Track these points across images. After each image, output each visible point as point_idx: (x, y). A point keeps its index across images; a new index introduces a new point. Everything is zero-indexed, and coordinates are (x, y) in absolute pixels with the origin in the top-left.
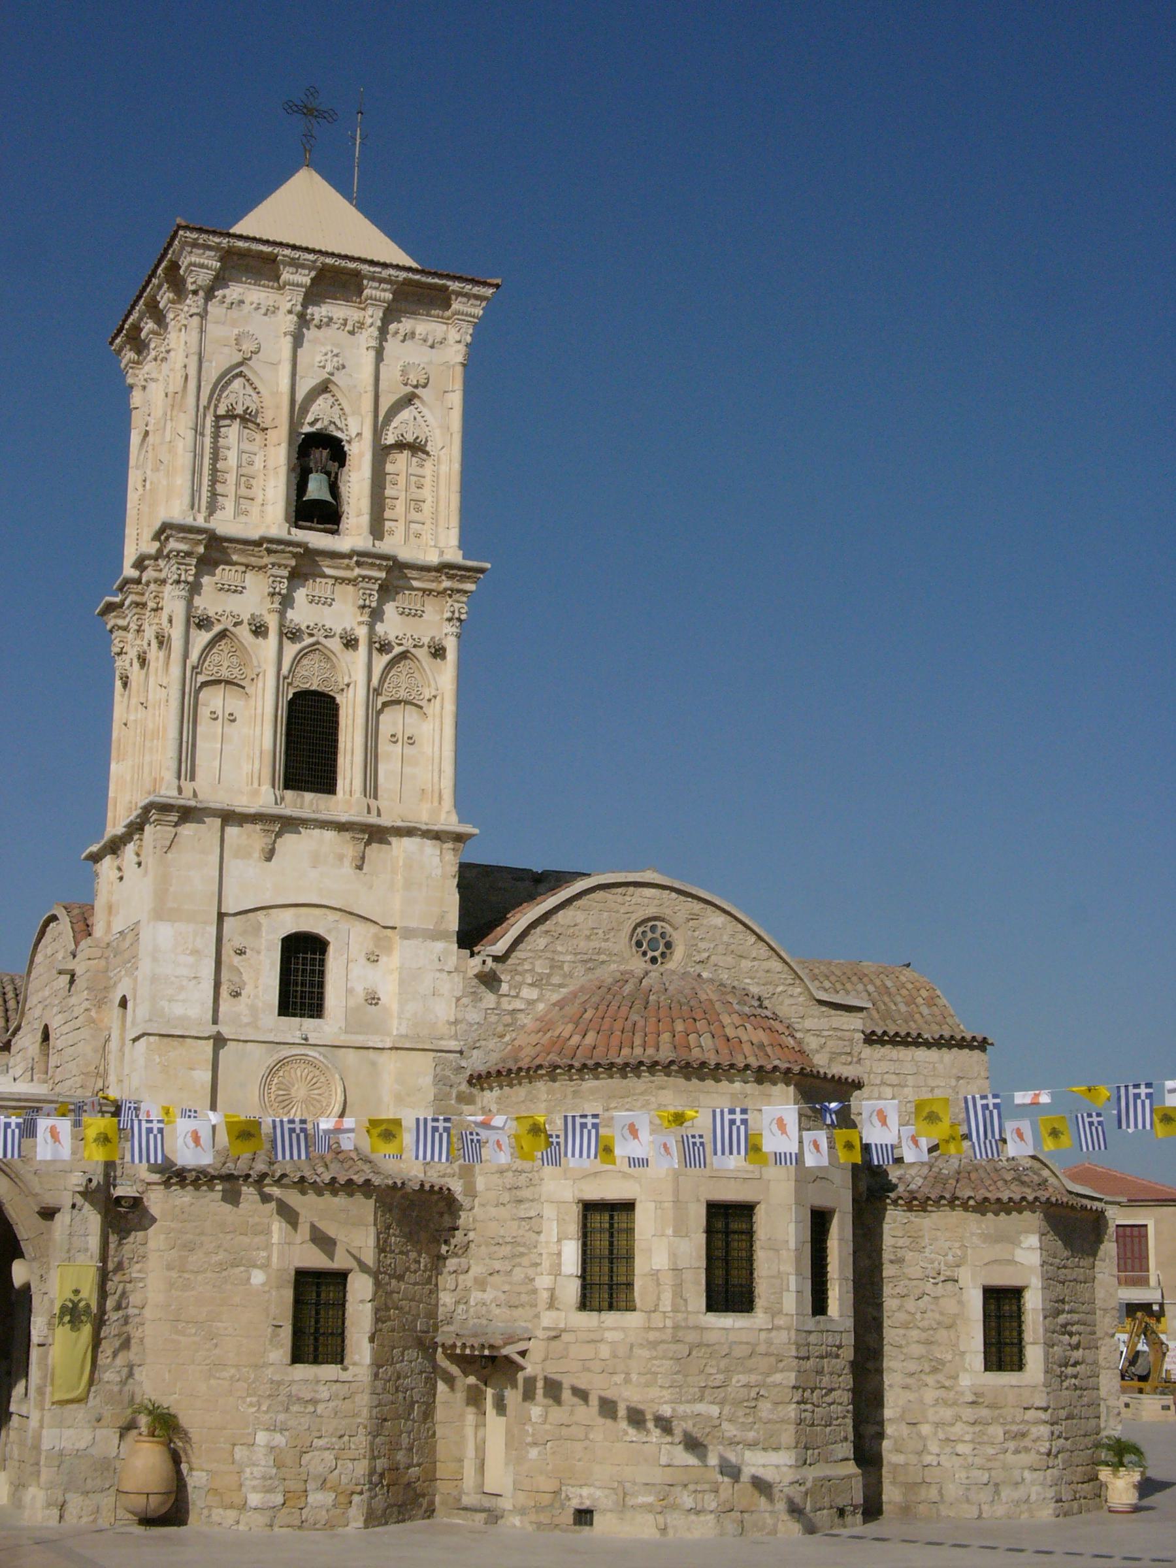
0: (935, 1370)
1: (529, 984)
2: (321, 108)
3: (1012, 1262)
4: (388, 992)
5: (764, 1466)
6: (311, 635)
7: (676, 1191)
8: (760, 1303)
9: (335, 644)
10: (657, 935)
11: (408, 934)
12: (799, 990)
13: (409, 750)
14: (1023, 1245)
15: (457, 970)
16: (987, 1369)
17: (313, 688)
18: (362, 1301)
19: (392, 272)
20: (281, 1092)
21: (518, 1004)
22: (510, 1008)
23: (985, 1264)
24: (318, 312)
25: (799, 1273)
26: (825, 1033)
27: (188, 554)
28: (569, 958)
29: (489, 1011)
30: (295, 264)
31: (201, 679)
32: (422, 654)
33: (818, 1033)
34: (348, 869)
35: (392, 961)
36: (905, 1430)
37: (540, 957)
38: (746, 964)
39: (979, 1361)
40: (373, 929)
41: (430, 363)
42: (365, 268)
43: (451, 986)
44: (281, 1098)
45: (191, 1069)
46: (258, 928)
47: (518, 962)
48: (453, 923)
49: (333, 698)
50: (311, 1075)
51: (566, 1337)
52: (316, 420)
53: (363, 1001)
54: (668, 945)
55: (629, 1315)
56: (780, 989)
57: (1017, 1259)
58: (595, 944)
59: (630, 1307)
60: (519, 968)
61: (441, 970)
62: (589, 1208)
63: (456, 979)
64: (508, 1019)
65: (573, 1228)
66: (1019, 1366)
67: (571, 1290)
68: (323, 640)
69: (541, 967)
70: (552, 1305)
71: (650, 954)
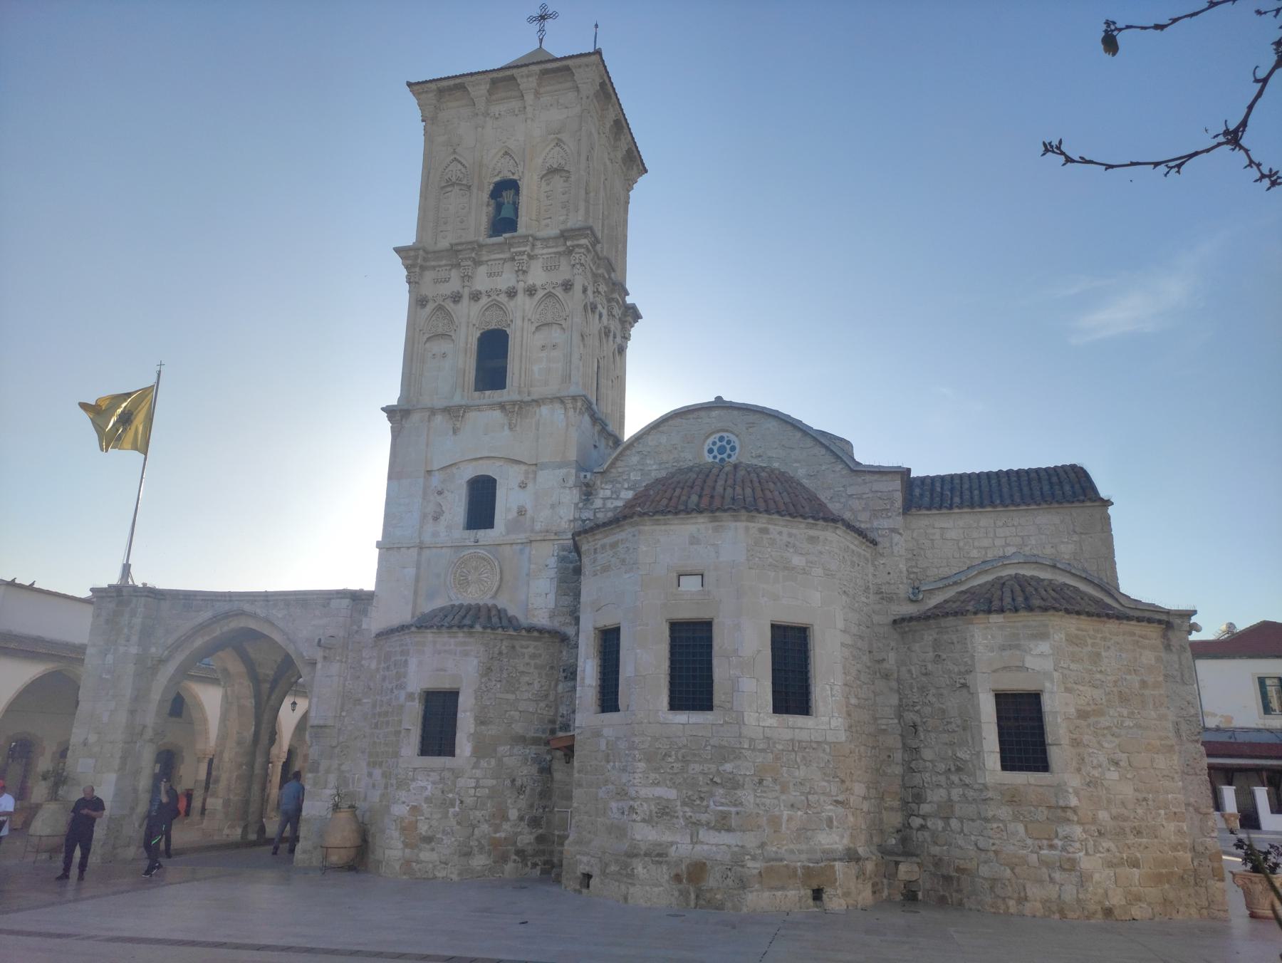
0: (959, 769)
1: (626, 489)
2: (549, 13)
3: (1022, 668)
5: (717, 845)
6: (489, 296)
8: (716, 701)
9: (503, 298)
10: (724, 443)
12: (841, 466)
14: (1034, 652)
15: (575, 486)
17: (493, 327)
18: (465, 711)
20: (462, 578)
22: (612, 506)
23: (994, 671)
24: (496, 109)
26: (865, 496)
28: (654, 467)
29: (597, 510)
31: (427, 336)
32: (559, 292)
33: (859, 496)
34: (507, 432)
36: (940, 824)
37: (634, 469)
40: (524, 468)
41: (568, 117)
42: (514, 71)
44: (462, 582)
45: (404, 568)
47: (618, 475)
49: (505, 331)
50: (482, 565)
52: (500, 172)
53: (516, 514)
54: (733, 449)
56: (823, 468)
57: (1027, 665)
60: (620, 479)
61: (565, 487)
63: (575, 492)
68: (496, 298)
71: (719, 457)
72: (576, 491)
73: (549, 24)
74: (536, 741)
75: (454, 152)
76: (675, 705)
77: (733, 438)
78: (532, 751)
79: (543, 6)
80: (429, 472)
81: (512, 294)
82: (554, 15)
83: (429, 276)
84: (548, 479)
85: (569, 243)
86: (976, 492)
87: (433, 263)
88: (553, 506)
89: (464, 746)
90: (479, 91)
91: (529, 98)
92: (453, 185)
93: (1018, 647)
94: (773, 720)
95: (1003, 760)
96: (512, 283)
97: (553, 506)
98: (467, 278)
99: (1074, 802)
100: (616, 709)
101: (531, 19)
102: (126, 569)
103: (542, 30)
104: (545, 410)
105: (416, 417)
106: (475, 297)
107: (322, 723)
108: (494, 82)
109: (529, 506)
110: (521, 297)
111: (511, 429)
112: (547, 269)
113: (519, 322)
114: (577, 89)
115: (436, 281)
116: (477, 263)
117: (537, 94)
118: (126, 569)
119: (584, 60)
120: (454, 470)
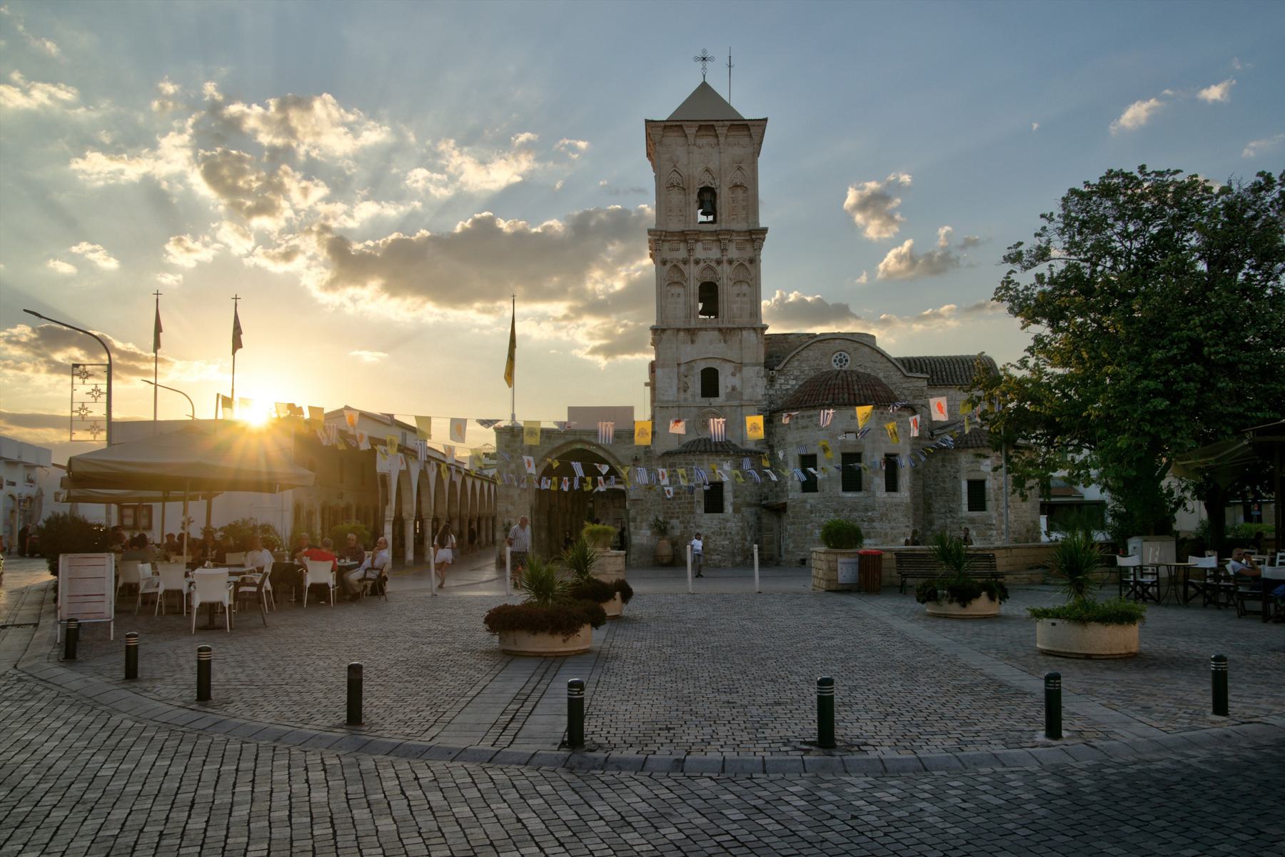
0: (950, 511)
3: (979, 471)
8: (863, 487)
9: (713, 264)
11: (746, 365)
13: (745, 299)
15: (765, 376)
16: (969, 510)
19: (725, 122)
21: (789, 387)
24: (701, 141)
27: (658, 240)
30: (687, 126)
34: (723, 344)
38: (878, 365)
39: (965, 508)
40: (733, 364)
46: (693, 367)
54: (846, 361)
55: (816, 494)
58: (817, 362)
59: (817, 491)
65: (798, 464)
66: (983, 508)
72: (765, 379)
73: (709, 64)
74: (755, 505)
75: (675, 166)
76: (844, 490)
77: (846, 355)
78: (753, 509)
79: (704, 51)
80: (679, 365)
81: (719, 262)
82: (712, 59)
83: (666, 246)
84: (749, 372)
85: (754, 237)
86: (944, 373)
87: (669, 238)
88: (753, 387)
89: (729, 508)
90: (691, 131)
91: (722, 139)
92: (674, 186)
93: (978, 462)
94: (885, 495)
95: (969, 507)
96: (719, 256)
97: (753, 387)
98: (690, 250)
99: (994, 522)
101: (696, 59)
102: (513, 416)
103: (704, 68)
104: (745, 333)
105: (669, 332)
106: (697, 262)
107: (636, 498)
108: (700, 127)
109: (738, 386)
110: (725, 265)
111: (725, 342)
112: (739, 249)
113: (725, 280)
114: (750, 136)
115: (671, 250)
116: (697, 241)
117: (727, 136)
118: (513, 416)
119: (757, 123)
120: (693, 364)
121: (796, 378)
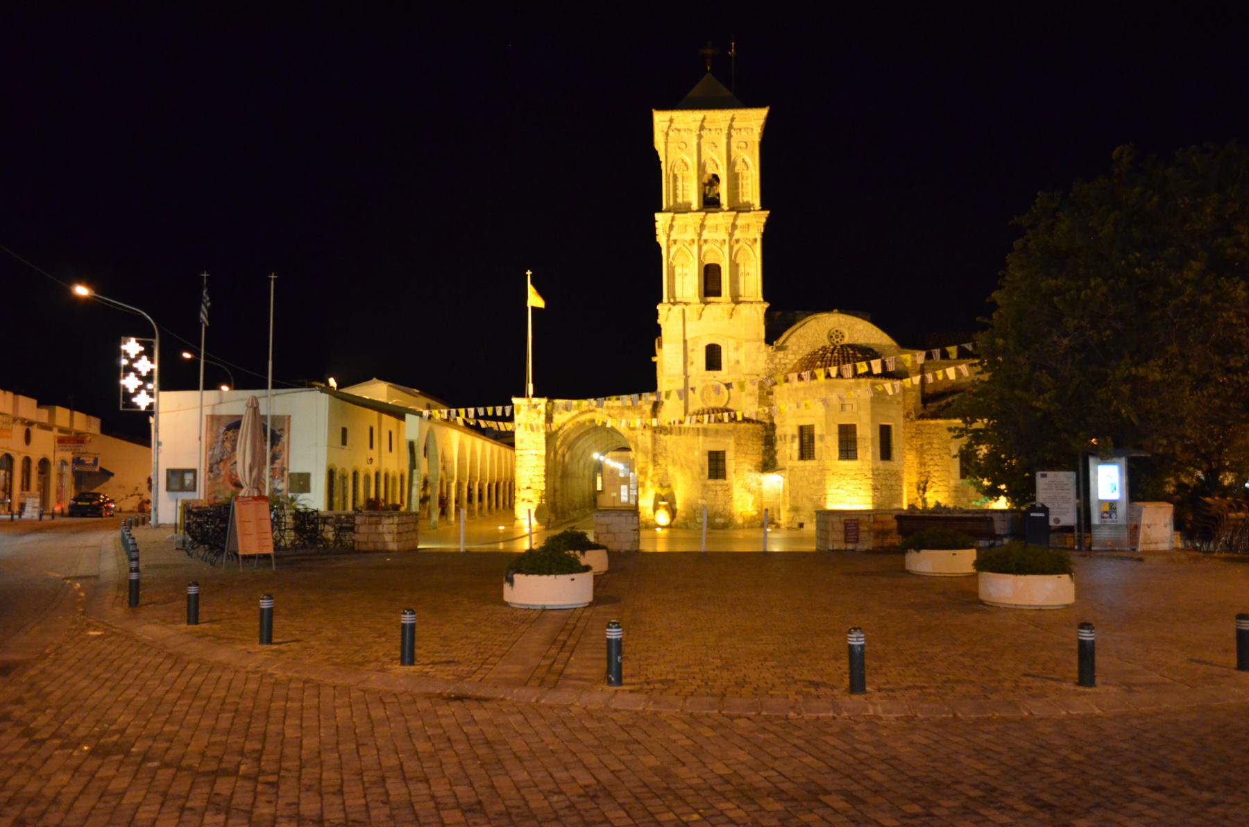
4: (742, 359)
7: (826, 419)
21: (787, 361)
25: (873, 444)
35: (743, 350)
43: (763, 357)
48: (763, 335)
51: (796, 469)
54: (843, 336)
62: (801, 428)
64: (783, 366)
67: (796, 454)
69: (795, 348)
70: (791, 458)
72: (765, 354)
100: (814, 458)
121: (794, 353)
